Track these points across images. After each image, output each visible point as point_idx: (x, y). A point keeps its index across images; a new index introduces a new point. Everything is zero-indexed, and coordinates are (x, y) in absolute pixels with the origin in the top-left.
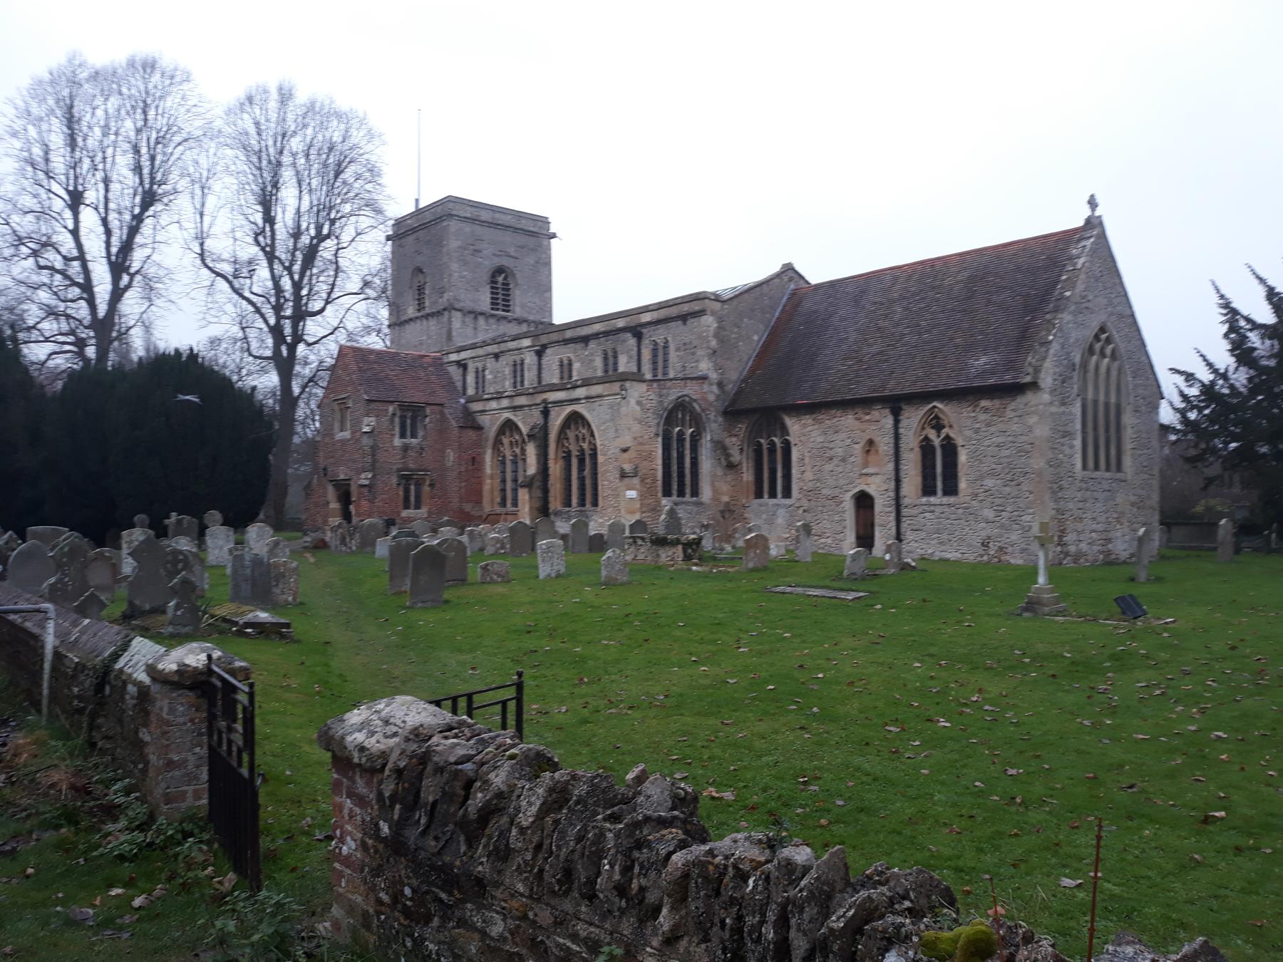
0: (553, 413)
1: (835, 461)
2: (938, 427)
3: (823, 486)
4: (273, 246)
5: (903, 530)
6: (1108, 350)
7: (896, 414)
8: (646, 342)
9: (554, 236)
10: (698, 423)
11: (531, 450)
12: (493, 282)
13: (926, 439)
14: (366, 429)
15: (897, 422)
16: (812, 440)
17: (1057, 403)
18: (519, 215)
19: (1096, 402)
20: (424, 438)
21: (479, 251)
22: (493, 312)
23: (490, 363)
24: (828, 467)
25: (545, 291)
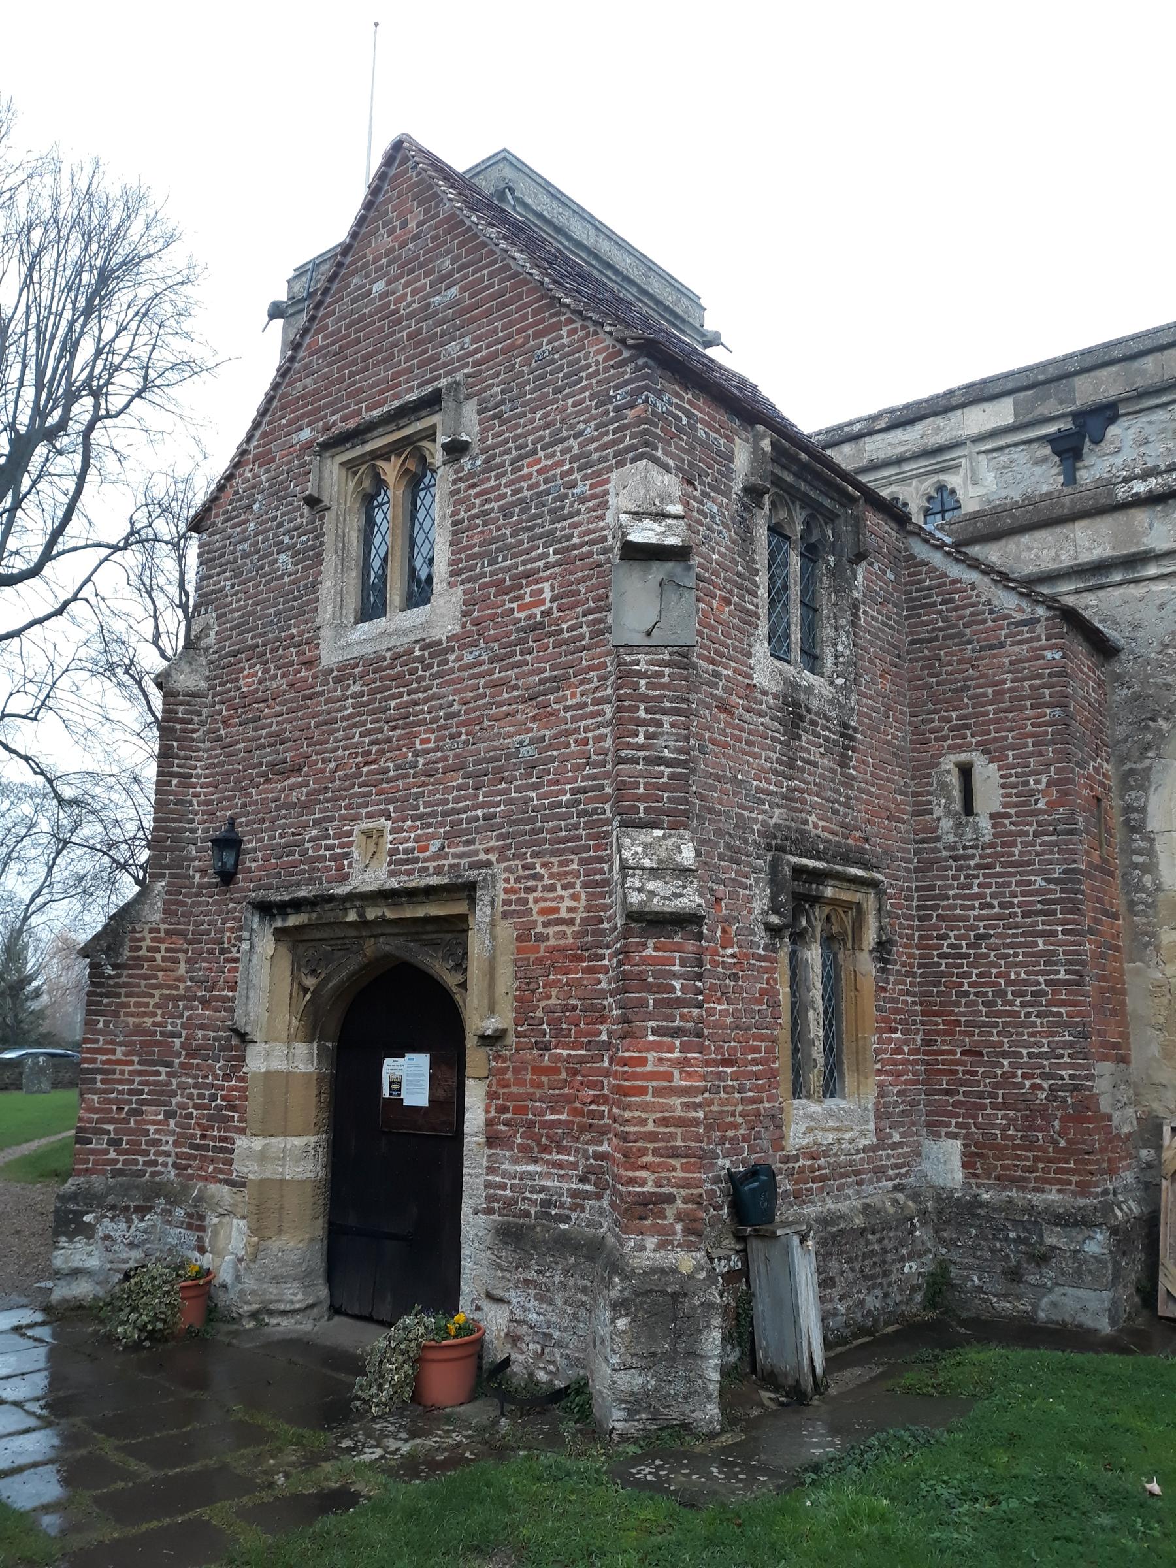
14: (645, 533)
20: (852, 667)
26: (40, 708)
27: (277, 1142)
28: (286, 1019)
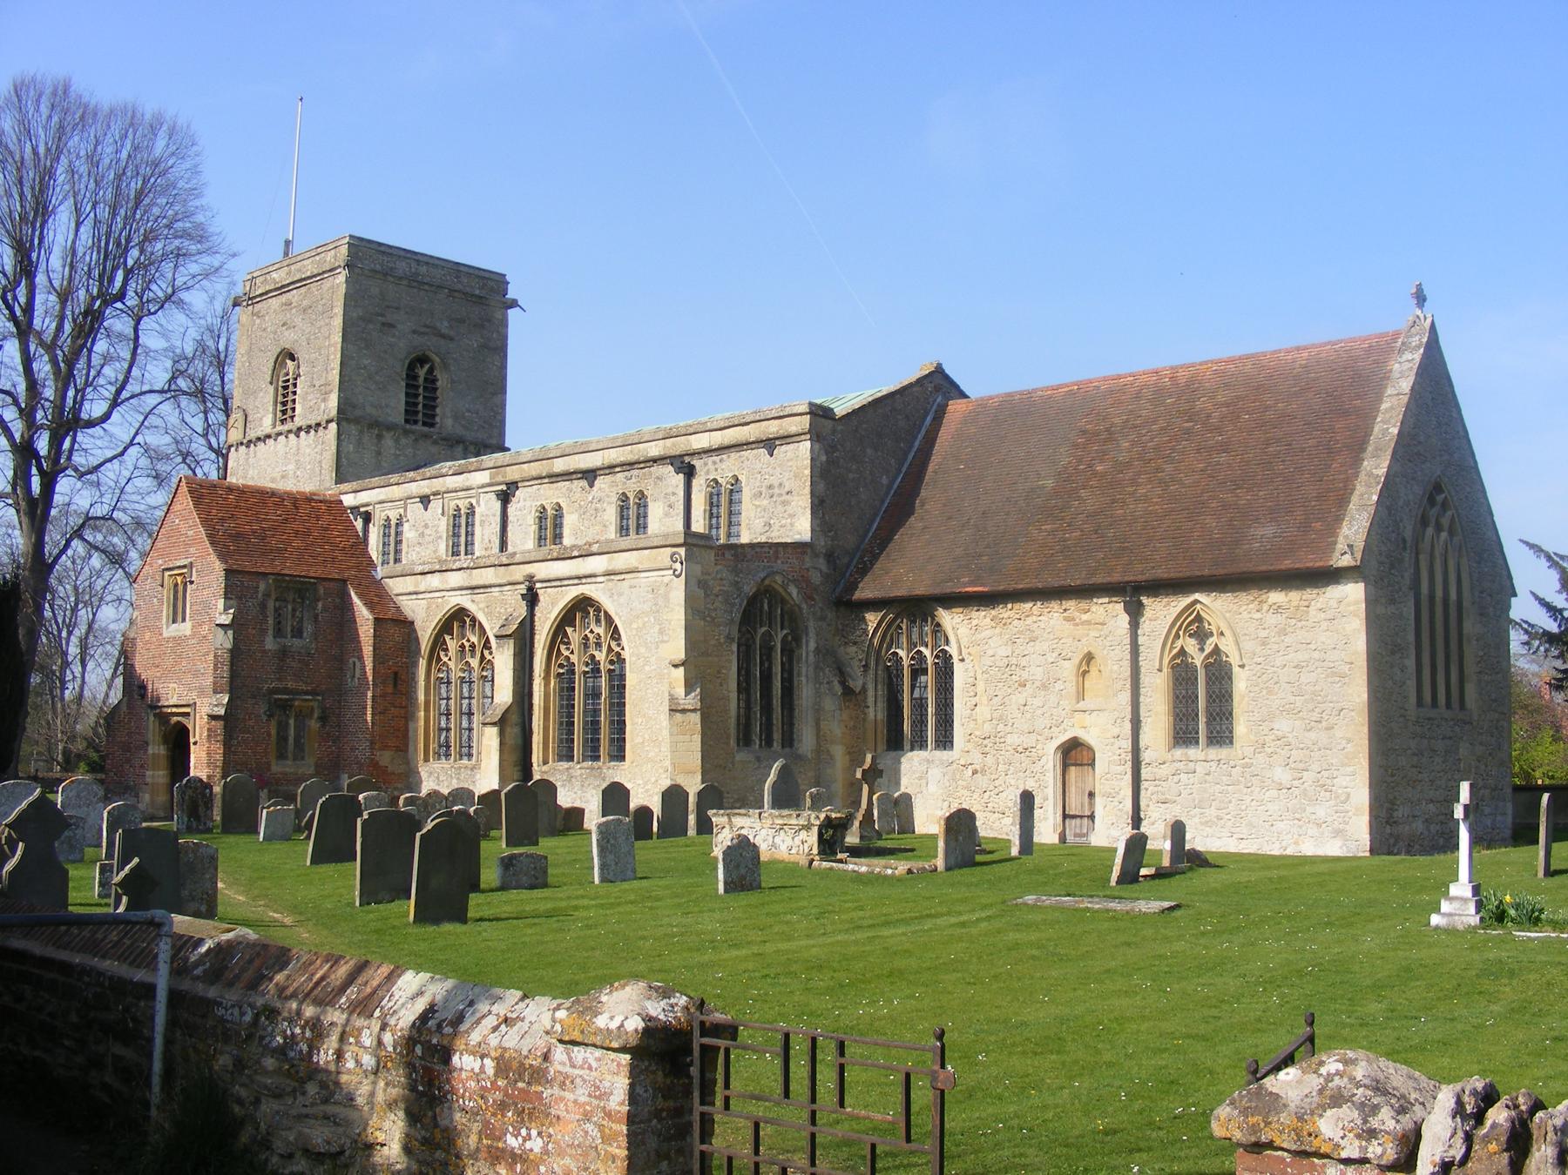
0: (544, 596)
1: (1029, 689)
2: (1201, 635)
3: (1009, 729)
4: (29, 309)
5: (1143, 804)
6: (1445, 522)
7: (1135, 612)
8: (699, 484)
9: (514, 304)
10: (792, 620)
11: (504, 661)
12: (411, 376)
13: (1182, 652)
15: (1134, 625)
16: (990, 652)
17: (1383, 600)
18: (457, 269)
19: (1432, 598)
20: (315, 636)
21: (391, 326)
22: (408, 426)
23: (415, 508)
24: (1019, 698)
25: (494, 394)
26: (113, 510)
27: (156, 773)
28: (158, 738)
